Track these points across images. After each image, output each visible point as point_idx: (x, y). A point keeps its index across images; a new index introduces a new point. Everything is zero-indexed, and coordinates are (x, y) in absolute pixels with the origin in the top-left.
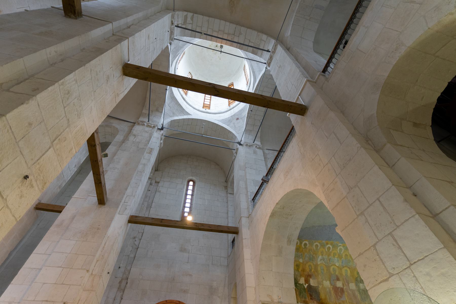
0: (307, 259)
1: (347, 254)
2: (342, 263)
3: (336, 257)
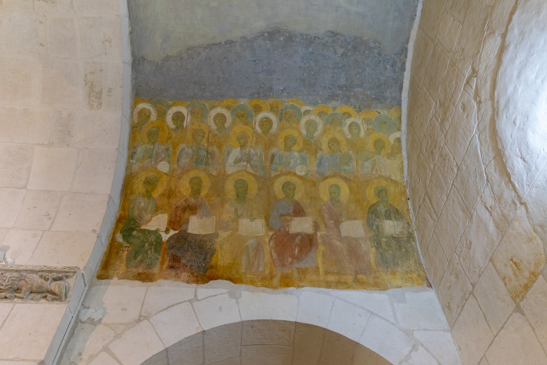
0: (185, 161)
1: (338, 136)
2: (319, 165)
3: (295, 148)
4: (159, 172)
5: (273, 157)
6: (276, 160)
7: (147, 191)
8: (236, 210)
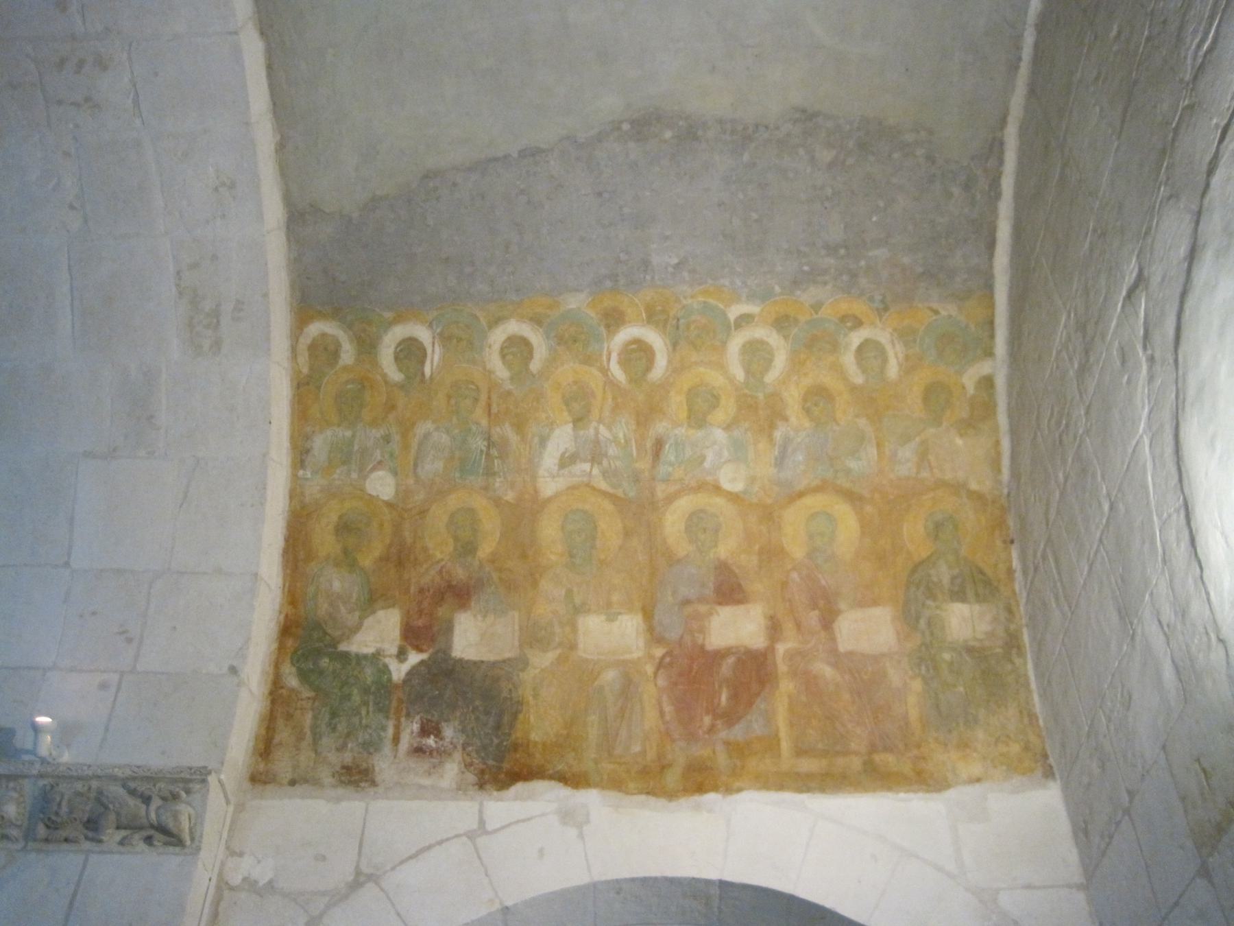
1: (829, 380)
2: (780, 462)
3: (720, 416)
4: (372, 499)
5: (659, 445)
6: (669, 453)
7: (345, 552)
8: (569, 592)
